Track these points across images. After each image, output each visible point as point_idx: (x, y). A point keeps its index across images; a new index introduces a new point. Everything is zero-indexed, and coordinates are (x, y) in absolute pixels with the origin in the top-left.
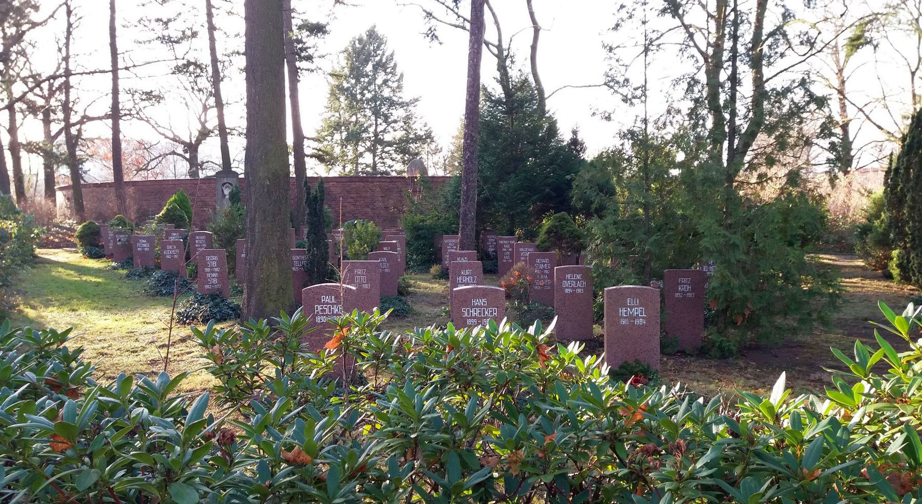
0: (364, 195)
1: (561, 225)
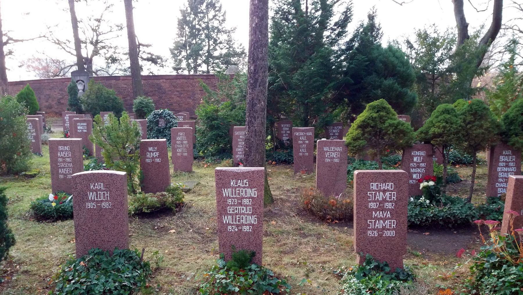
0: (186, 89)
1: (381, 117)
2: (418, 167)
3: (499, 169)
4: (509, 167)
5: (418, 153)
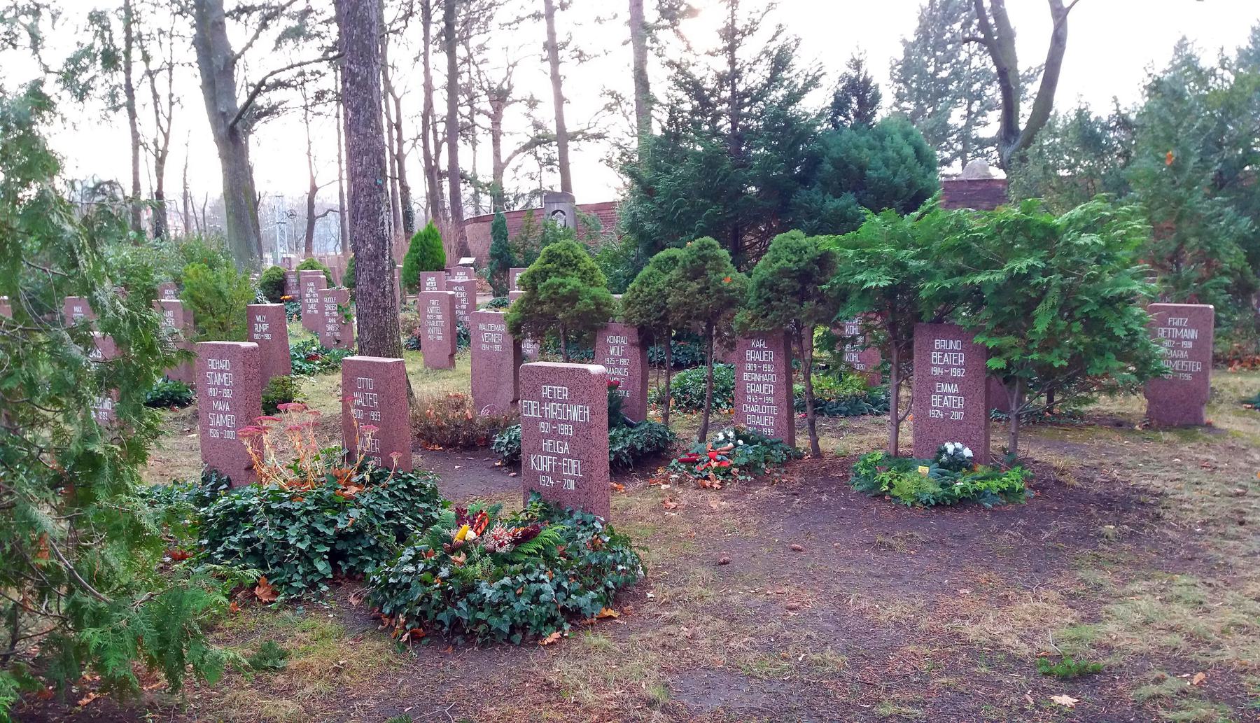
2: (618, 365)
3: (746, 376)
5: (616, 339)
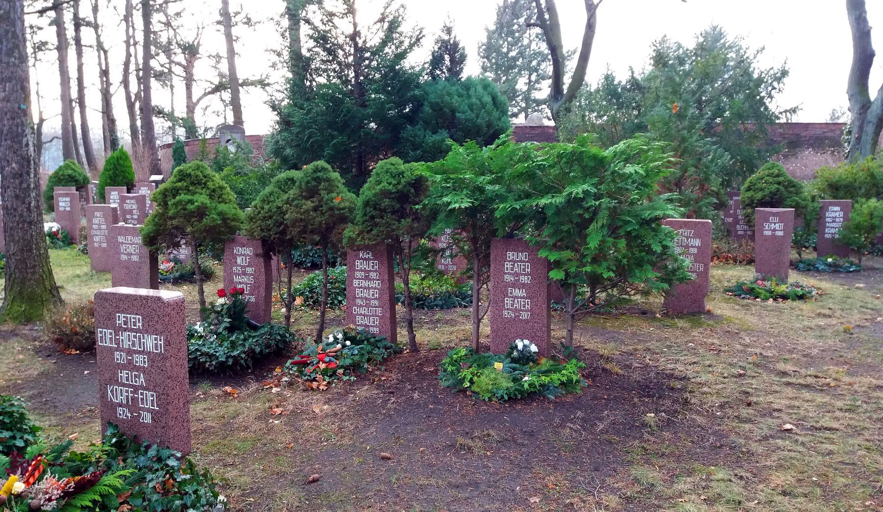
2: (244, 274)
3: (356, 283)
4: (370, 280)
5: (242, 250)
